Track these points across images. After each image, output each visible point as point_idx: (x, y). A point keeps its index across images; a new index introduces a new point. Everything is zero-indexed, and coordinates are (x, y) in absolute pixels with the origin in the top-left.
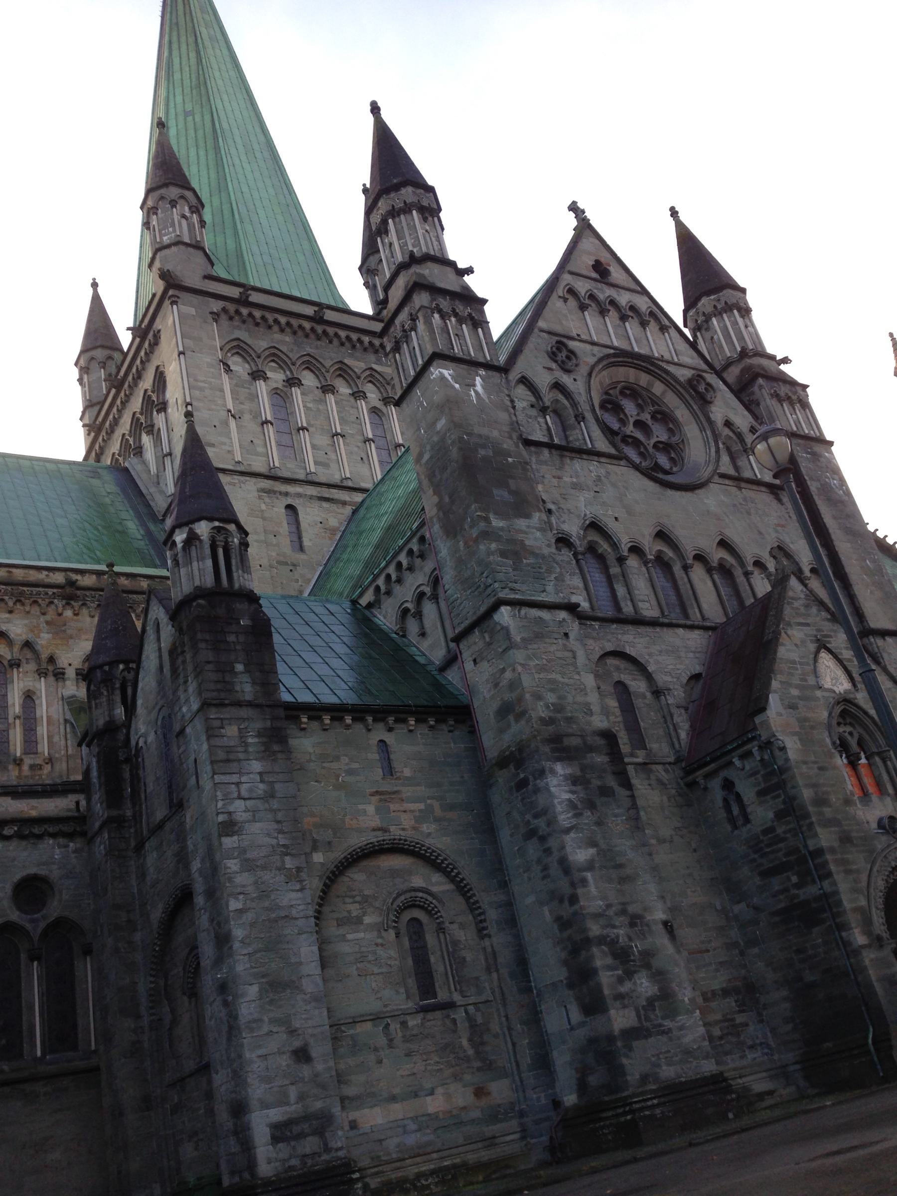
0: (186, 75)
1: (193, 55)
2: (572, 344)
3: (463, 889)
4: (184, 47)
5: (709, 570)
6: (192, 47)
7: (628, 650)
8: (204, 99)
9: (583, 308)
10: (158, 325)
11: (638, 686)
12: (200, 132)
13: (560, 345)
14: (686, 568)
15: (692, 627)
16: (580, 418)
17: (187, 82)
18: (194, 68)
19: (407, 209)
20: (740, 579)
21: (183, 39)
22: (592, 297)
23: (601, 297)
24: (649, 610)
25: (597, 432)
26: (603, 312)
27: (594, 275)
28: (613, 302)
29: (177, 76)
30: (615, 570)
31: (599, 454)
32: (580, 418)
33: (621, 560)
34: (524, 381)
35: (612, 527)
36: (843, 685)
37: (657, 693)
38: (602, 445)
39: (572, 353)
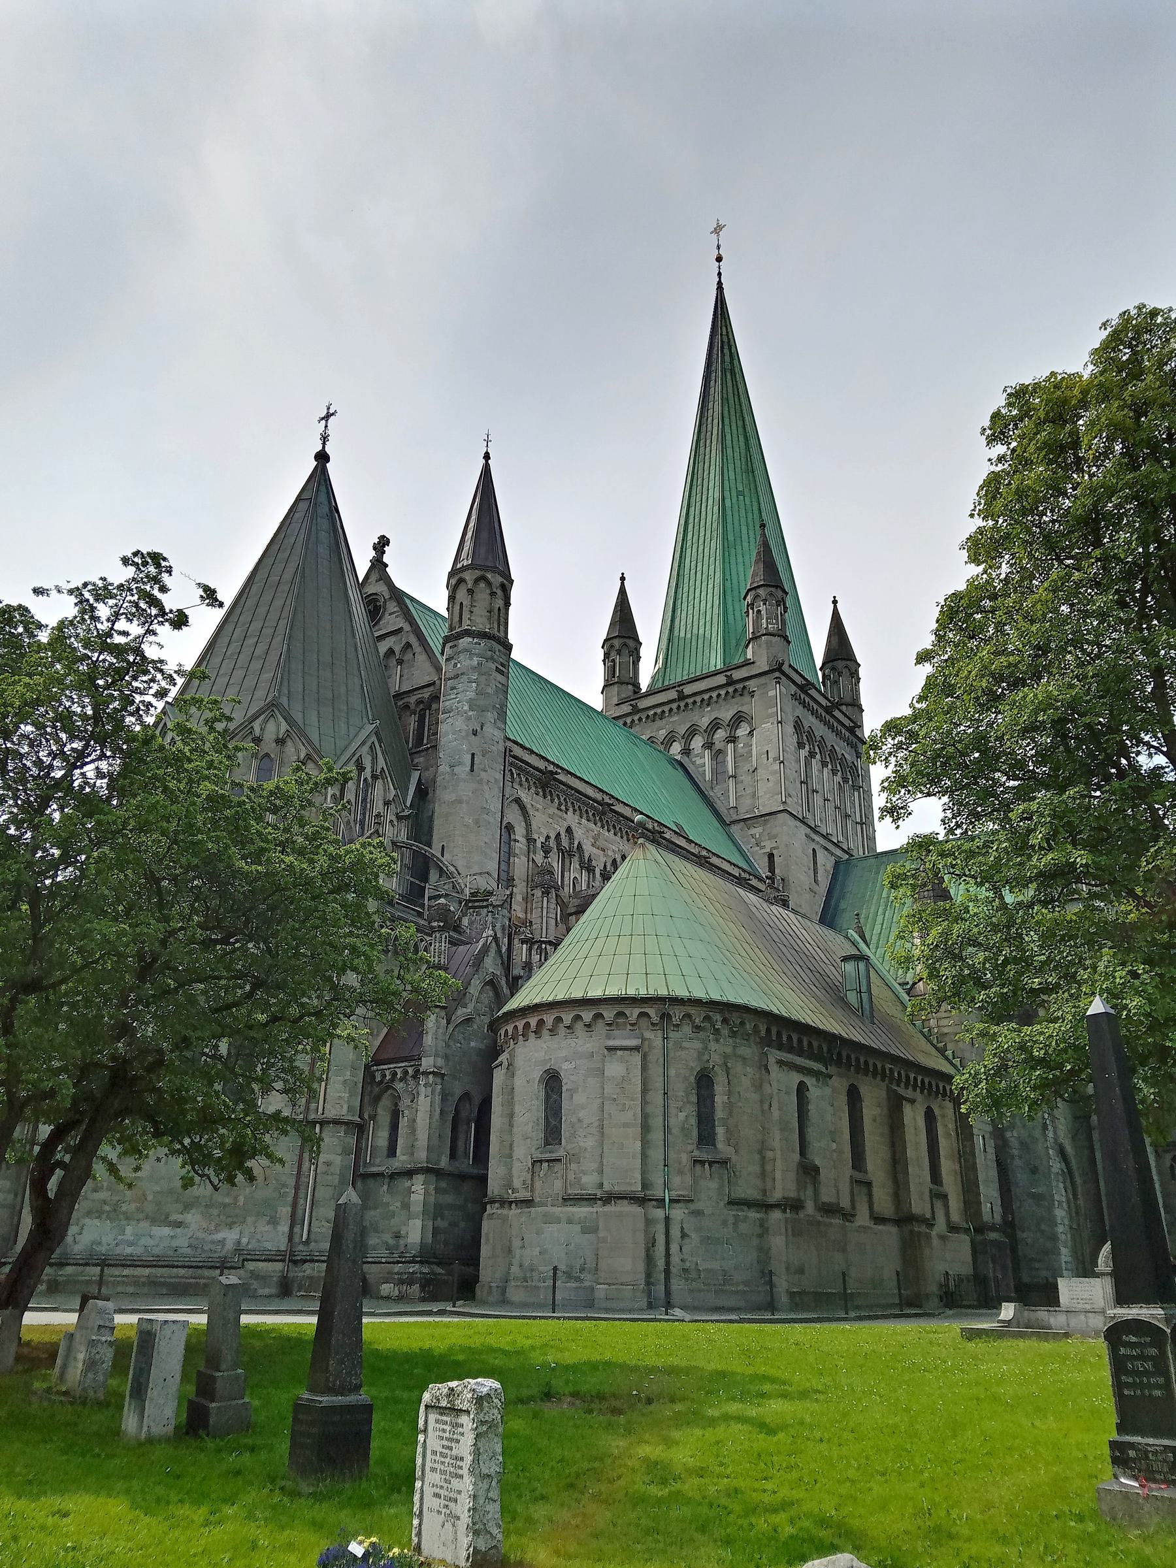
0: (737, 455)
1: (742, 439)
4: (734, 425)
6: (741, 430)
8: (752, 485)
10: (752, 684)
12: (750, 515)
17: (738, 462)
18: (743, 451)
21: (733, 418)
29: (729, 451)
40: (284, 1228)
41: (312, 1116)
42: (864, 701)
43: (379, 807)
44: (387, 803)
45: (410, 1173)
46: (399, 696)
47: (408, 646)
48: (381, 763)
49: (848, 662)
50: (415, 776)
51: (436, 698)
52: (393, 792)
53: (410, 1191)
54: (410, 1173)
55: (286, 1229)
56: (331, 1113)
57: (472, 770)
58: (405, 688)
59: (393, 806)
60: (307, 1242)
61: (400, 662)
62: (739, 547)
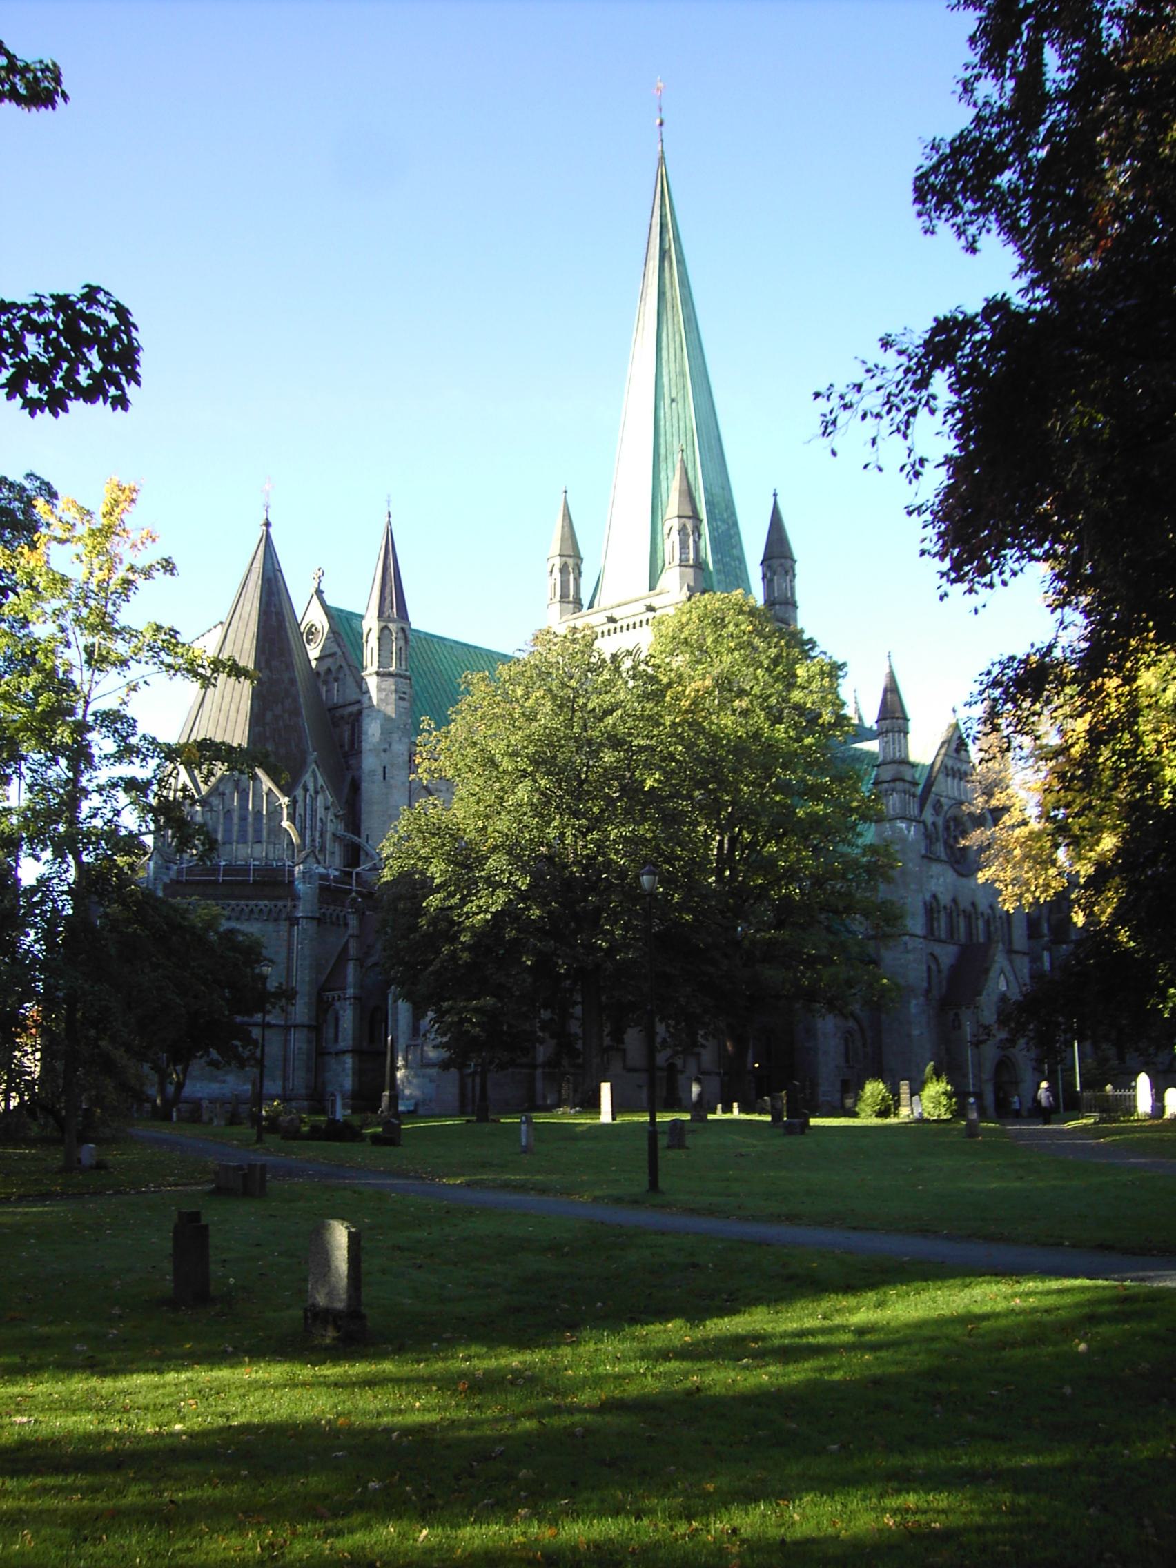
2: (942, 799)
3: (862, 1029)
5: (965, 916)
7: (935, 953)
9: (947, 775)
11: (934, 967)
13: (939, 801)
14: (958, 915)
15: (954, 944)
16: (937, 840)
19: (899, 732)
20: (973, 920)
22: (952, 768)
23: (956, 768)
24: (943, 936)
25: (942, 849)
26: (954, 777)
27: (955, 755)
28: (959, 770)
30: (935, 915)
31: (942, 861)
32: (937, 840)
33: (939, 912)
34: (924, 822)
35: (940, 896)
36: (1004, 989)
37: (939, 971)
38: (943, 856)
39: (941, 806)
40: (280, 1083)
41: (289, 1023)
42: (800, 597)
43: (321, 812)
44: (327, 808)
45: (344, 1052)
46: (337, 707)
47: (341, 667)
48: (321, 781)
49: (783, 561)
50: (349, 778)
51: (360, 712)
52: (331, 800)
53: (345, 1063)
54: (344, 1052)
55: (281, 1083)
56: (298, 1022)
57: (384, 778)
58: (341, 702)
59: (332, 809)
60: (292, 1090)
61: (336, 680)
62: (669, 460)
